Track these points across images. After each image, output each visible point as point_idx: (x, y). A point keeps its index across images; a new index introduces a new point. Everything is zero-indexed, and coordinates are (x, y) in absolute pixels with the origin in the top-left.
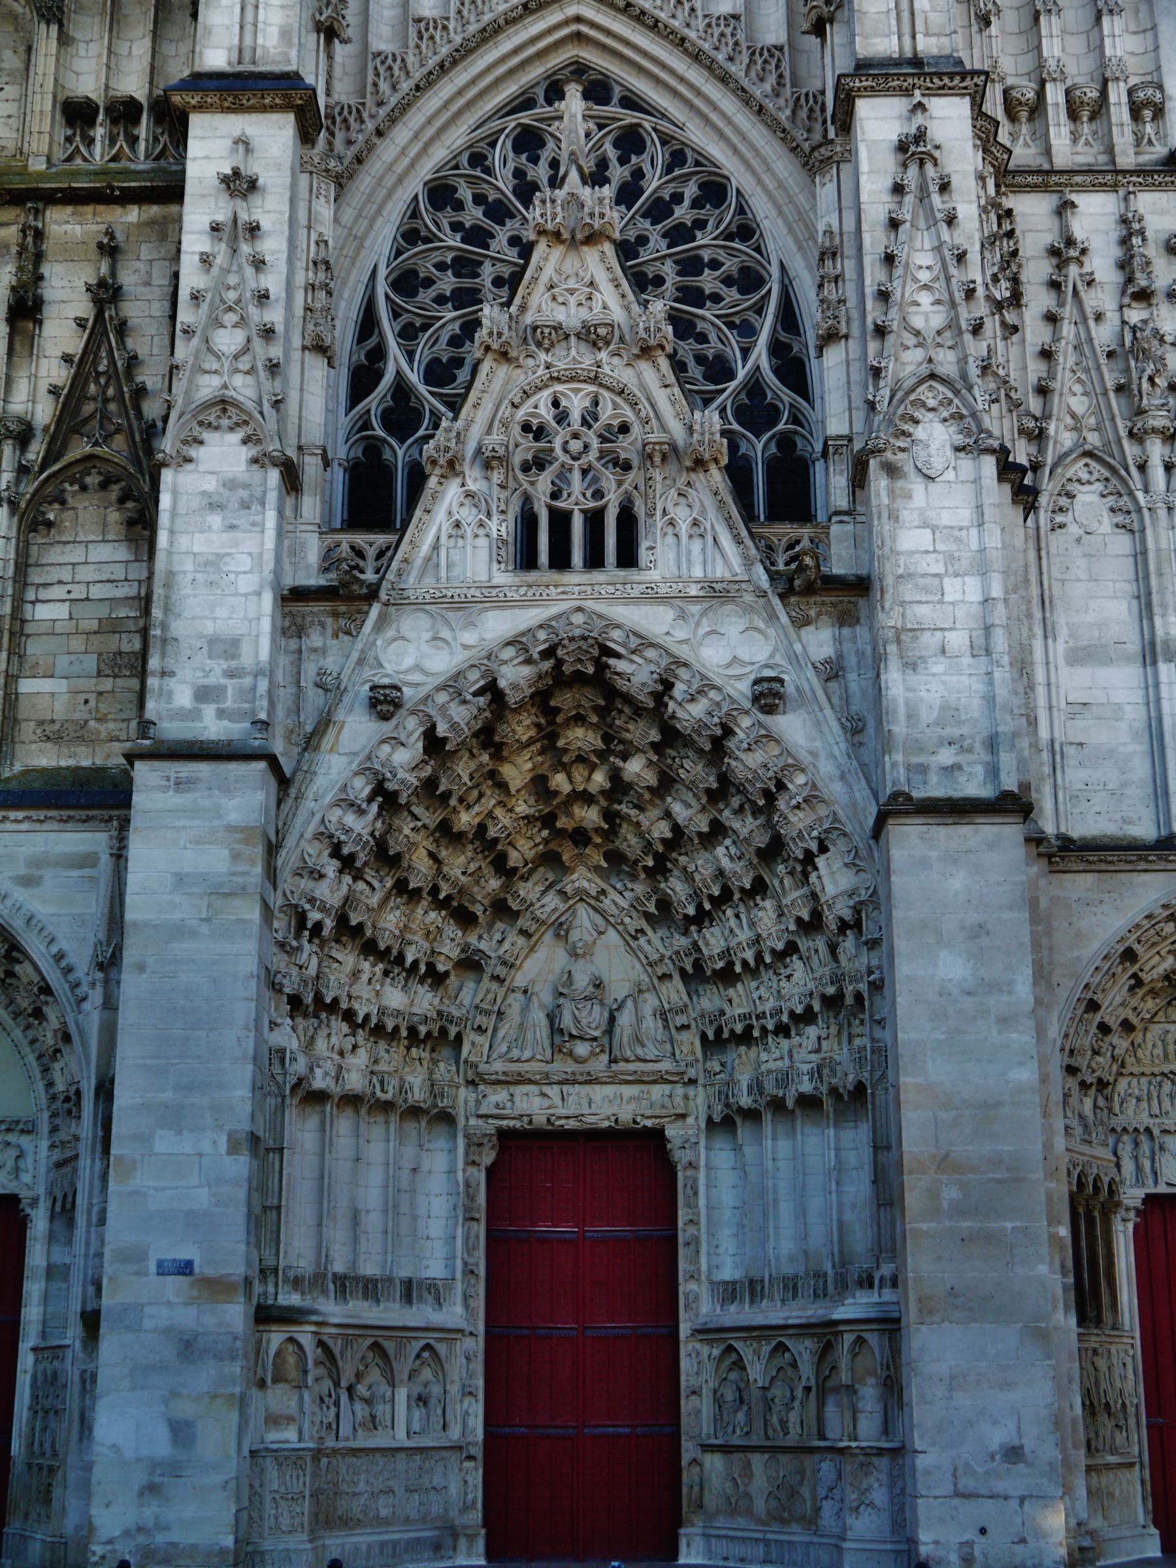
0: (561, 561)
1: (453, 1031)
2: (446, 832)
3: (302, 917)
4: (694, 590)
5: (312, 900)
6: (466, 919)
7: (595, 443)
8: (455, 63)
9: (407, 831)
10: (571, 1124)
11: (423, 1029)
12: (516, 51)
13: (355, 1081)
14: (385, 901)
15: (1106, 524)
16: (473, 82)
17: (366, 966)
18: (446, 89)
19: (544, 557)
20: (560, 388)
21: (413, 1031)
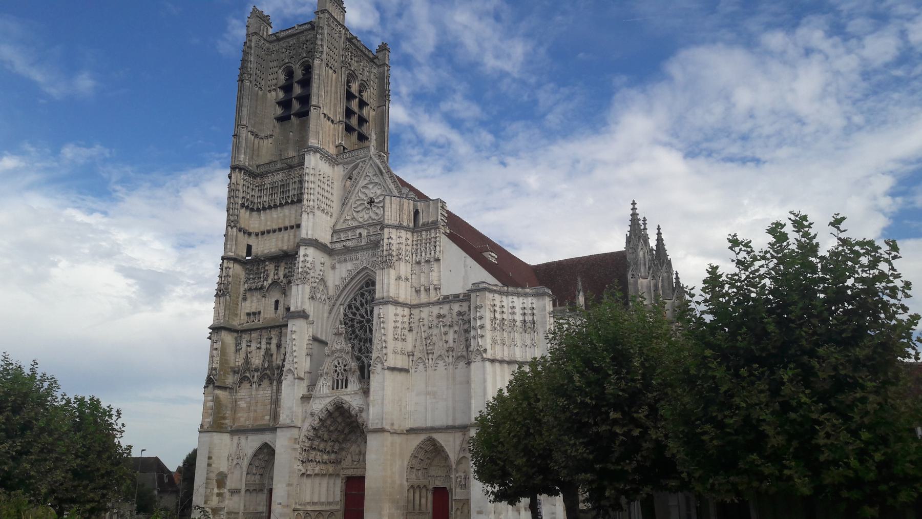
0: (337, 388)
1: (339, 460)
2: (330, 432)
3: (303, 448)
4: (353, 393)
5: (304, 446)
6: (339, 442)
7: (342, 367)
8: (348, 285)
9: (321, 432)
10: (355, 476)
11: (332, 461)
12: (358, 280)
13: (316, 472)
14: (320, 443)
15: (423, 371)
16: (352, 286)
17: (318, 453)
18: (347, 289)
19: (335, 388)
20: (338, 359)
21: (330, 462)
